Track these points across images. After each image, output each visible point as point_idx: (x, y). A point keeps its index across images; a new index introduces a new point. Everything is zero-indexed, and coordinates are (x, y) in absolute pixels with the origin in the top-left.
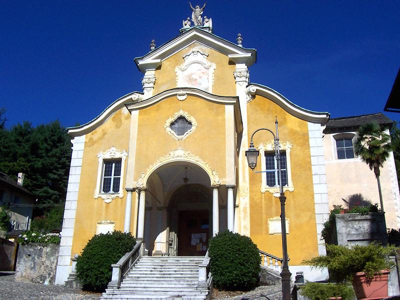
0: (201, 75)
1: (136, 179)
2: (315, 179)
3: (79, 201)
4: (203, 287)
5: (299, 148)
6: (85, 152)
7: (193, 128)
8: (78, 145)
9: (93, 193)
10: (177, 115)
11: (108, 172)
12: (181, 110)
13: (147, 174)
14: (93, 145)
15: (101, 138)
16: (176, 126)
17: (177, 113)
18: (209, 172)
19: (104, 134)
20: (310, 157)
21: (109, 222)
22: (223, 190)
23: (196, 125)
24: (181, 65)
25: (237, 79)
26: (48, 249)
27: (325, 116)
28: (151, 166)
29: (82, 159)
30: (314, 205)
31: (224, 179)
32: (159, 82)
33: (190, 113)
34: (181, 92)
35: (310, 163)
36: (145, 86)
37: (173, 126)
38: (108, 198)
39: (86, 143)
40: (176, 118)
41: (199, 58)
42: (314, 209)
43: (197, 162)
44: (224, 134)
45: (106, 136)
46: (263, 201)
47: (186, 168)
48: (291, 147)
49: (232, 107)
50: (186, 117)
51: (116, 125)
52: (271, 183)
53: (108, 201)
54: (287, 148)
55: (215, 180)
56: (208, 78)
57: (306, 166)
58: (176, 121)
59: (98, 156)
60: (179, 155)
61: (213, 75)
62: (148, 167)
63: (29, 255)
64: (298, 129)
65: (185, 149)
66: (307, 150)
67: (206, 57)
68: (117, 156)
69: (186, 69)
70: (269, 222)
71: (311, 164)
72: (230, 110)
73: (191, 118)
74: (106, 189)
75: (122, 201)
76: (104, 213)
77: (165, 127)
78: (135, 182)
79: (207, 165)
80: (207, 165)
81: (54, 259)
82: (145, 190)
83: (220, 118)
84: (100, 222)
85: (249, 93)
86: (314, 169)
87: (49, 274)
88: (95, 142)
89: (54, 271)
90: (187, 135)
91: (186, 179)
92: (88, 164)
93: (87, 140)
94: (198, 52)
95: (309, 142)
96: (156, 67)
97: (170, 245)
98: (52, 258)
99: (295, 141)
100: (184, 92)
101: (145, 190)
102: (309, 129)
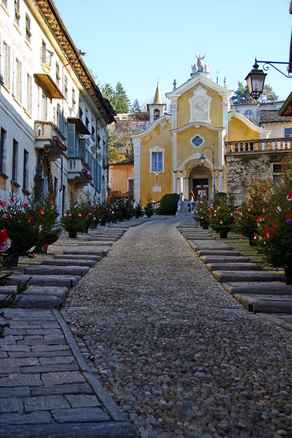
0: (203, 104)
7: (203, 142)
10: (196, 135)
14: (145, 144)
15: (150, 140)
19: (151, 138)
32: (180, 107)
45: (152, 139)
56: (207, 106)
76: (155, 181)
88: (146, 143)
92: (144, 154)
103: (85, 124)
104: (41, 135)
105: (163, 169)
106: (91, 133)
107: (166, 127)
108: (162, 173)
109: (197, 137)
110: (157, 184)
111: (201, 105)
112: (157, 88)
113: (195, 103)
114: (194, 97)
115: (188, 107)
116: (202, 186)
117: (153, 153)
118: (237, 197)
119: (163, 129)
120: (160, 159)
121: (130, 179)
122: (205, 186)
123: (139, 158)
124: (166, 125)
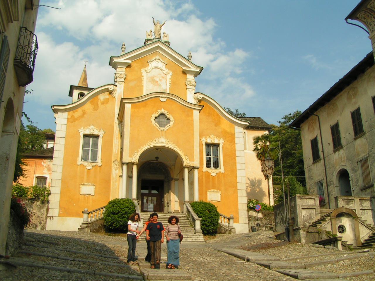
1: (131, 155)
2: (238, 166)
3: (64, 166)
4: (199, 233)
5: (228, 143)
6: (68, 127)
7: (171, 123)
9: (76, 161)
10: (160, 112)
11: (86, 145)
12: (163, 109)
13: (139, 154)
17: (159, 111)
18: (183, 156)
20: (235, 150)
21: (90, 184)
22: (191, 169)
23: (174, 121)
24: (146, 68)
25: (188, 87)
27: (247, 124)
28: (142, 148)
29: (65, 132)
30: (237, 184)
31: (193, 162)
32: (129, 78)
33: (170, 113)
34: (163, 96)
35: (235, 154)
36: (117, 80)
37: (157, 120)
38: (89, 165)
39: (68, 119)
40: (159, 114)
41: (160, 65)
42: (237, 186)
43: (174, 148)
44: (193, 130)
45: (85, 116)
46: (204, 177)
47: (157, 150)
48: (223, 142)
50: (166, 114)
51: (94, 108)
52: (208, 165)
53: (89, 168)
54: (221, 143)
55: (186, 162)
56: (166, 82)
57: (232, 156)
58: (159, 116)
59: (80, 131)
60: (162, 142)
61: (170, 80)
62: (139, 147)
64: (228, 130)
65: (166, 138)
66: (234, 146)
67: (165, 65)
68: (96, 132)
69: (150, 72)
70: (208, 193)
71: (235, 155)
73: (169, 116)
74: (85, 159)
76: (85, 177)
77: (151, 120)
78: (130, 158)
79: (182, 151)
80: (182, 151)
81: (44, 211)
82: (137, 165)
84: (83, 184)
86: (238, 160)
87: (40, 223)
88: (77, 119)
89: (45, 221)
90: (167, 128)
91: (157, 158)
92: (70, 137)
93: (69, 117)
94: (159, 60)
95: (235, 140)
96: (127, 66)
98: (42, 210)
99: (226, 138)
100: (165, 96)
101: (137, 165)
102: (235, 131)
105: (99, 160)
107: (106, 101)
109: (162, 114)
110: (88, 181)
111: (158, 80)
112: (85, 71)
114: (149, 68)
115: (140, 79)
116: (150, 192)
119: (103, 103)
120: (95, 145)
121: (37, 175)
122: (154, 192)
123: (63, 141)
124: (108, 99)
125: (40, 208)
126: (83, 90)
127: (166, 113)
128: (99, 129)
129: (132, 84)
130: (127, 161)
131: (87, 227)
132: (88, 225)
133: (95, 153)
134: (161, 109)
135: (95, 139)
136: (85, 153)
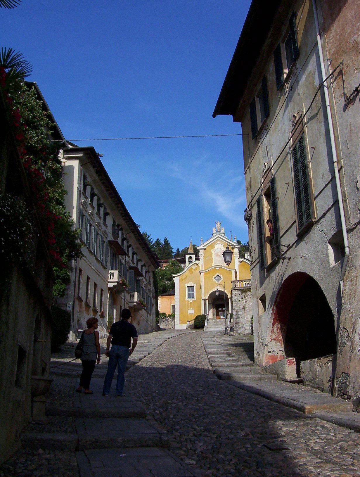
7: (222, 279)
8: (177, 280)
9: (185, 299)
10: (216, 275)
11: (189, 291)
12: (218, 273)
16: (216, 278)
19: (186, 277)
26: (171, 319)
32: (205, 256)
33: (221, 274)
38: (191, 300)
39: (180, 280)
45: (187, 277)
49: (234, 272)
63: (164, 321)
68: (192, 285)
72: (233, 273)
74: (189, 297)
75: (196, 302)
76: (190, 306)
82: (208, 299)
83: (230, 276)
85: (239, 261)
88: (183, 280)
97: (214, 316)
98: (172, 322)
101: (208, 299)
103: (140, 270)
104: (112, 279)
106: (144, 276)
107: (196, 269)
108: (194, 300)
109: (218, 275)
110: (191, 308)
113: (216, 252)
114: (215, 248)
117: (188, 287)
118: (240, 317)
119: (194, 270)
120: (193, 291)
124: (197, 268)
125: (171, 321)
126: (191, 255)
127: (219, 274)
128: (194, 282)
129: (207, 258)
130: (204, 299)
131: (189, 327)
132: (189, 326)
133: (193, 294)
134: (217, 273)
135: (193, 288)
136: (189, 295)
